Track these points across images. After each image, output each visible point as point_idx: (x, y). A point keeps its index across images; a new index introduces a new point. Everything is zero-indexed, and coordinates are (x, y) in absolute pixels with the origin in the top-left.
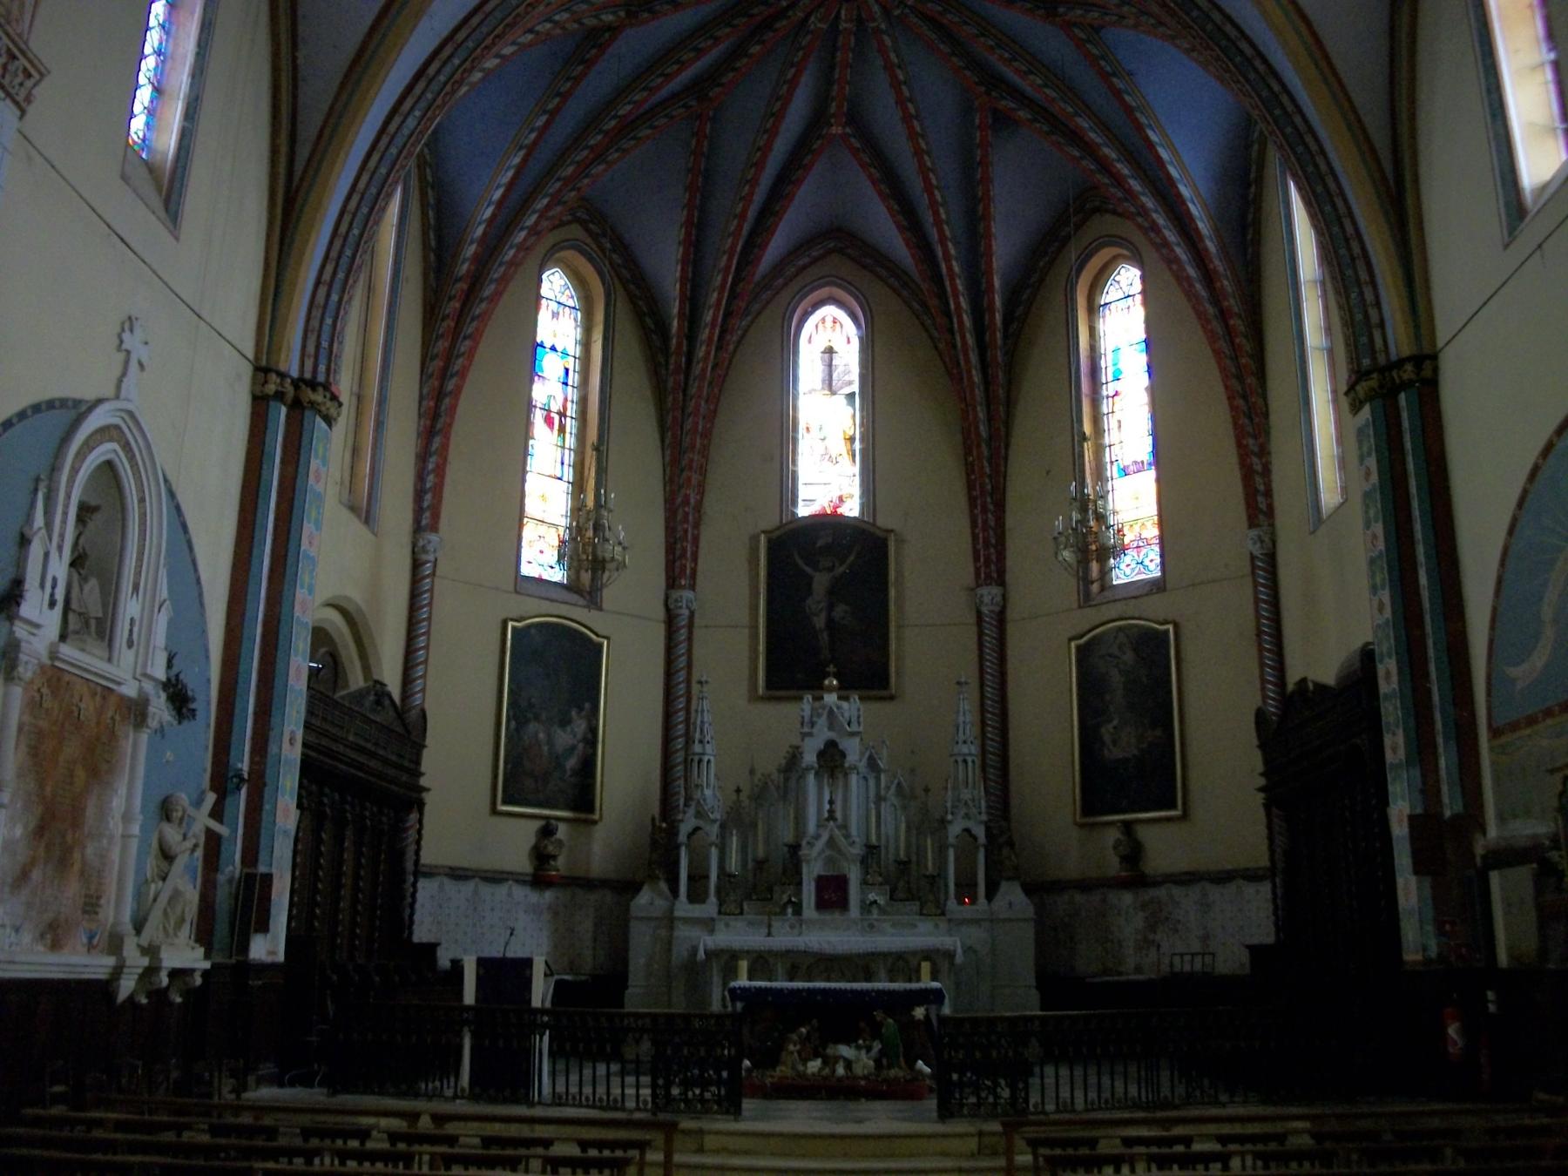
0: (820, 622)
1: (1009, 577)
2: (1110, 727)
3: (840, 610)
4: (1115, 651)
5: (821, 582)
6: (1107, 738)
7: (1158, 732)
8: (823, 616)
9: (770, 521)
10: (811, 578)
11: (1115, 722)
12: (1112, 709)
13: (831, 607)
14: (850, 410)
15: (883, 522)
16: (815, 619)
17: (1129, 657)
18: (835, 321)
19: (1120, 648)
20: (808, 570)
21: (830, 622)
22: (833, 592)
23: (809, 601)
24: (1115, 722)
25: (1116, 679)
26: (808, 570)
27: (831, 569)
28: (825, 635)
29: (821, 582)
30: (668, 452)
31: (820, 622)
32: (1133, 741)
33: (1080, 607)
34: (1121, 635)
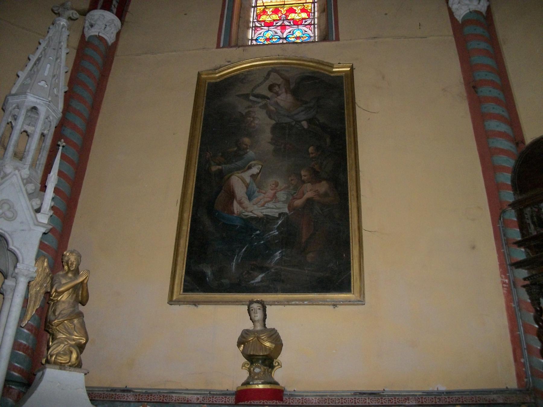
1: (128, 17)
2: (247, 176)
4: (263, 90)
6: (240, 190)
7: (323, 187)
11: (255, 170)
12: (251, 153)
17: (284, 99)
19: (271, 88)
24: (255, 170)
25: (262, 121)
32: (282, 196)
33: (218, 46)
34: (273, 75)
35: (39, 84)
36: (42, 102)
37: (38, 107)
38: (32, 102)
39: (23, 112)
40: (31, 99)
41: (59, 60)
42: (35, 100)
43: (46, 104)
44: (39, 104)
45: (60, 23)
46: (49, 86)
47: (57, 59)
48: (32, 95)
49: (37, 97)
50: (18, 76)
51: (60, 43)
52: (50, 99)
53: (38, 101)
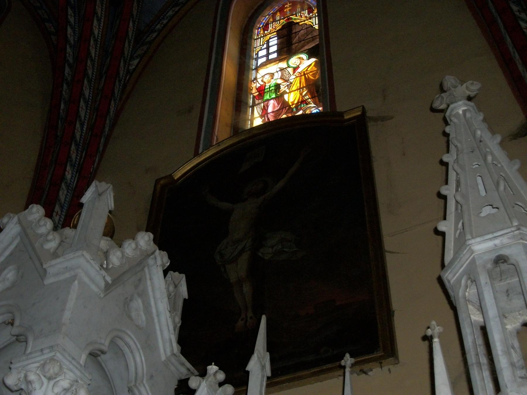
15: (348, 106)
20: (225, 205)
26: (225, 205)
35: (482, 215)
36: (505, 240)
37: (505, 252)
38: (489, 251)
39: (483, 279)
40: (482, 246)
41: (489, 158)
42: (489, 245)
43: (514, 237)
44: (503, 246)
45: (457, 115)
46: (501, 205)
47: (485, 159)
48: (478, 239)
49: (490, 236)
50: (443, 234)
51: (474, 135)
52: (516, 224)
53: (497, 242)
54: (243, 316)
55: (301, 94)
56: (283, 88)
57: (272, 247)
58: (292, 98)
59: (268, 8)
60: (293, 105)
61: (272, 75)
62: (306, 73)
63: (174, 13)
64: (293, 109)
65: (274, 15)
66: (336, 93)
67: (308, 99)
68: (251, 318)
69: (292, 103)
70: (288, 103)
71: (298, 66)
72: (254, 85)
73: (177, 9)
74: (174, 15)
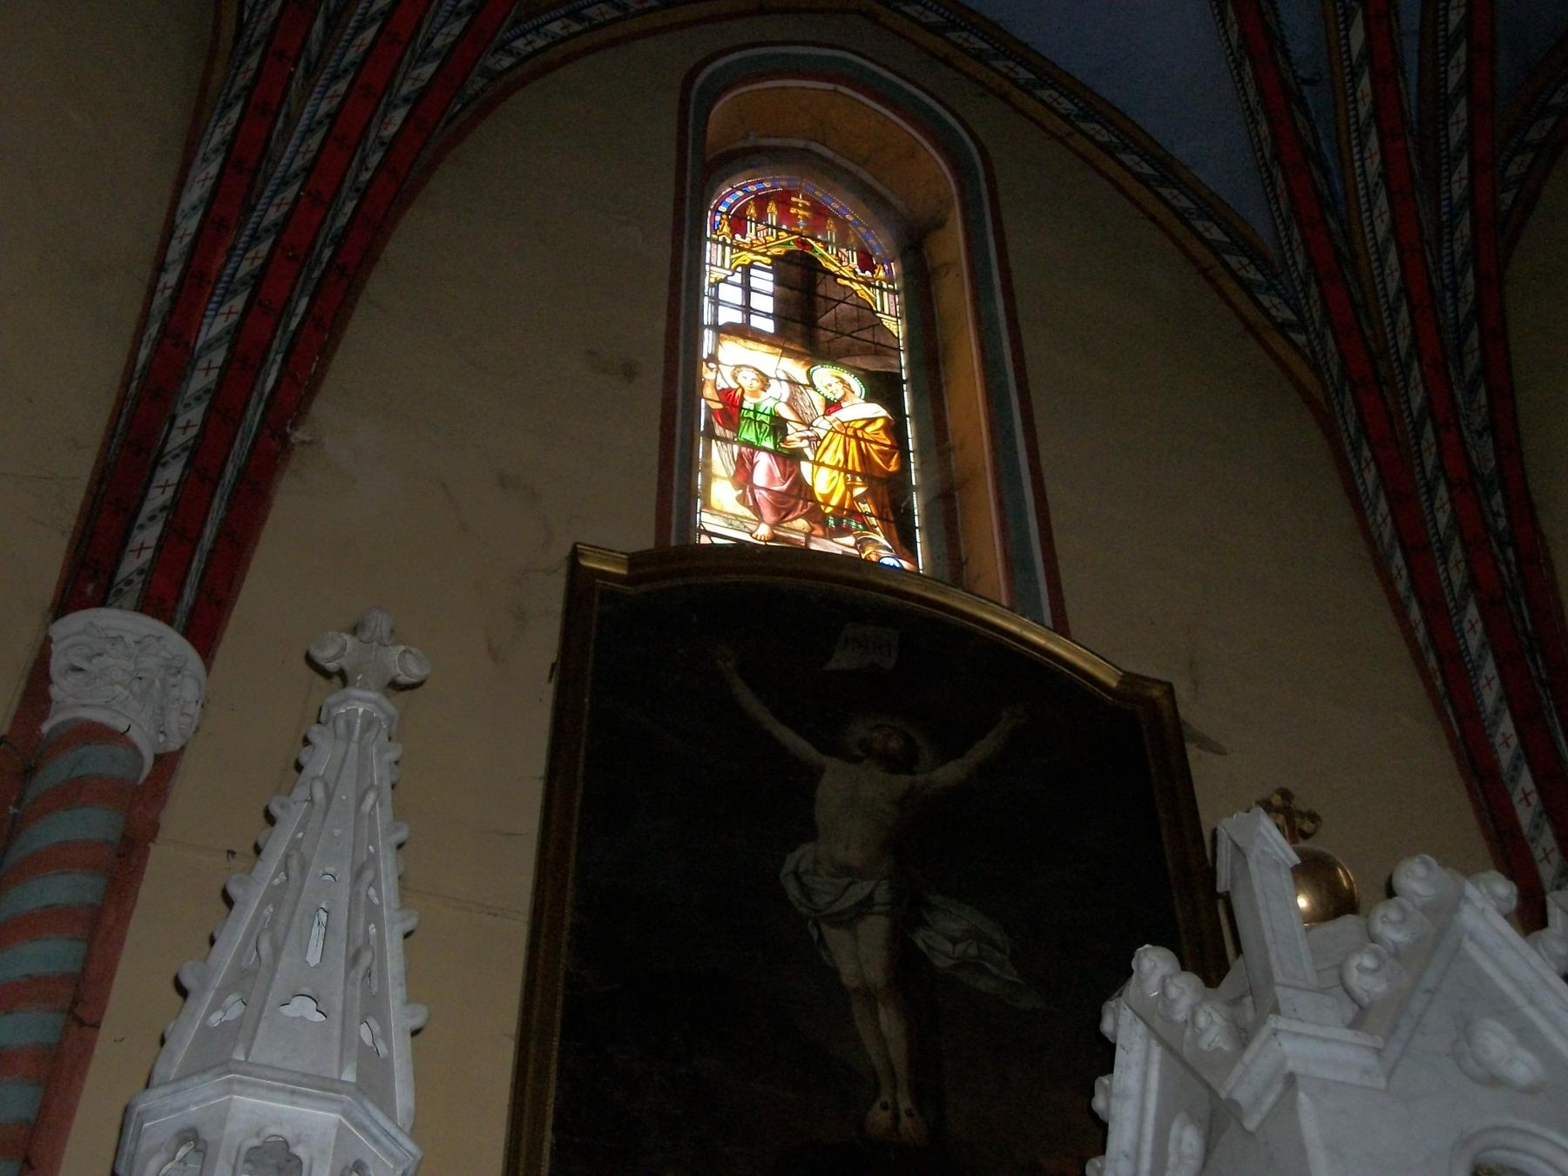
0: (860, 955)
3: (949, 935)
5: (852, 801)
8: (875, 928)
9: (619, 538)
10: (813, 774)
13: (908, 915)
14: (876, 410)
16: (836, 938)
18: (819, 212)
21: (907, 965)
22: (925, 852)
23: (802, 856)
27: (903, 763)
28: (890, 1022)
29: (852, 801)
30: (206, 173)
31: (860, 955)
54: (885, 1097)
55: (849, 488)
56: (795, 436)
57: (954, 941)
58: (826, 482)
59: (749, 172)
60: (827, 505)
61: (765, 381)
62: (859, 433)
63: (564, 33)
64: (825, 516)
65: (761, 201)
66: (1067, 593)
67: (871, 515)
68: (909, 1113)
69: (823, 496)
70: (810, 490)
71: (839, 401)
72: (708, 375)
73: (576, 27)
74: (563, 40)
